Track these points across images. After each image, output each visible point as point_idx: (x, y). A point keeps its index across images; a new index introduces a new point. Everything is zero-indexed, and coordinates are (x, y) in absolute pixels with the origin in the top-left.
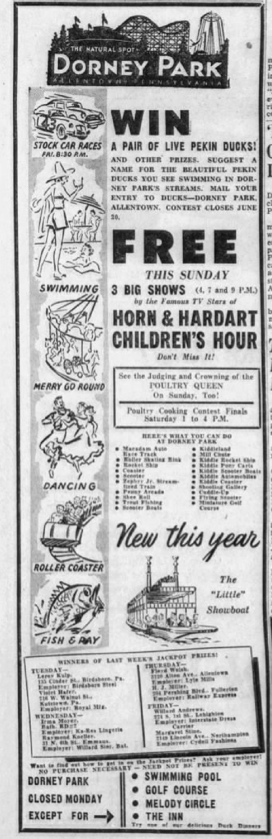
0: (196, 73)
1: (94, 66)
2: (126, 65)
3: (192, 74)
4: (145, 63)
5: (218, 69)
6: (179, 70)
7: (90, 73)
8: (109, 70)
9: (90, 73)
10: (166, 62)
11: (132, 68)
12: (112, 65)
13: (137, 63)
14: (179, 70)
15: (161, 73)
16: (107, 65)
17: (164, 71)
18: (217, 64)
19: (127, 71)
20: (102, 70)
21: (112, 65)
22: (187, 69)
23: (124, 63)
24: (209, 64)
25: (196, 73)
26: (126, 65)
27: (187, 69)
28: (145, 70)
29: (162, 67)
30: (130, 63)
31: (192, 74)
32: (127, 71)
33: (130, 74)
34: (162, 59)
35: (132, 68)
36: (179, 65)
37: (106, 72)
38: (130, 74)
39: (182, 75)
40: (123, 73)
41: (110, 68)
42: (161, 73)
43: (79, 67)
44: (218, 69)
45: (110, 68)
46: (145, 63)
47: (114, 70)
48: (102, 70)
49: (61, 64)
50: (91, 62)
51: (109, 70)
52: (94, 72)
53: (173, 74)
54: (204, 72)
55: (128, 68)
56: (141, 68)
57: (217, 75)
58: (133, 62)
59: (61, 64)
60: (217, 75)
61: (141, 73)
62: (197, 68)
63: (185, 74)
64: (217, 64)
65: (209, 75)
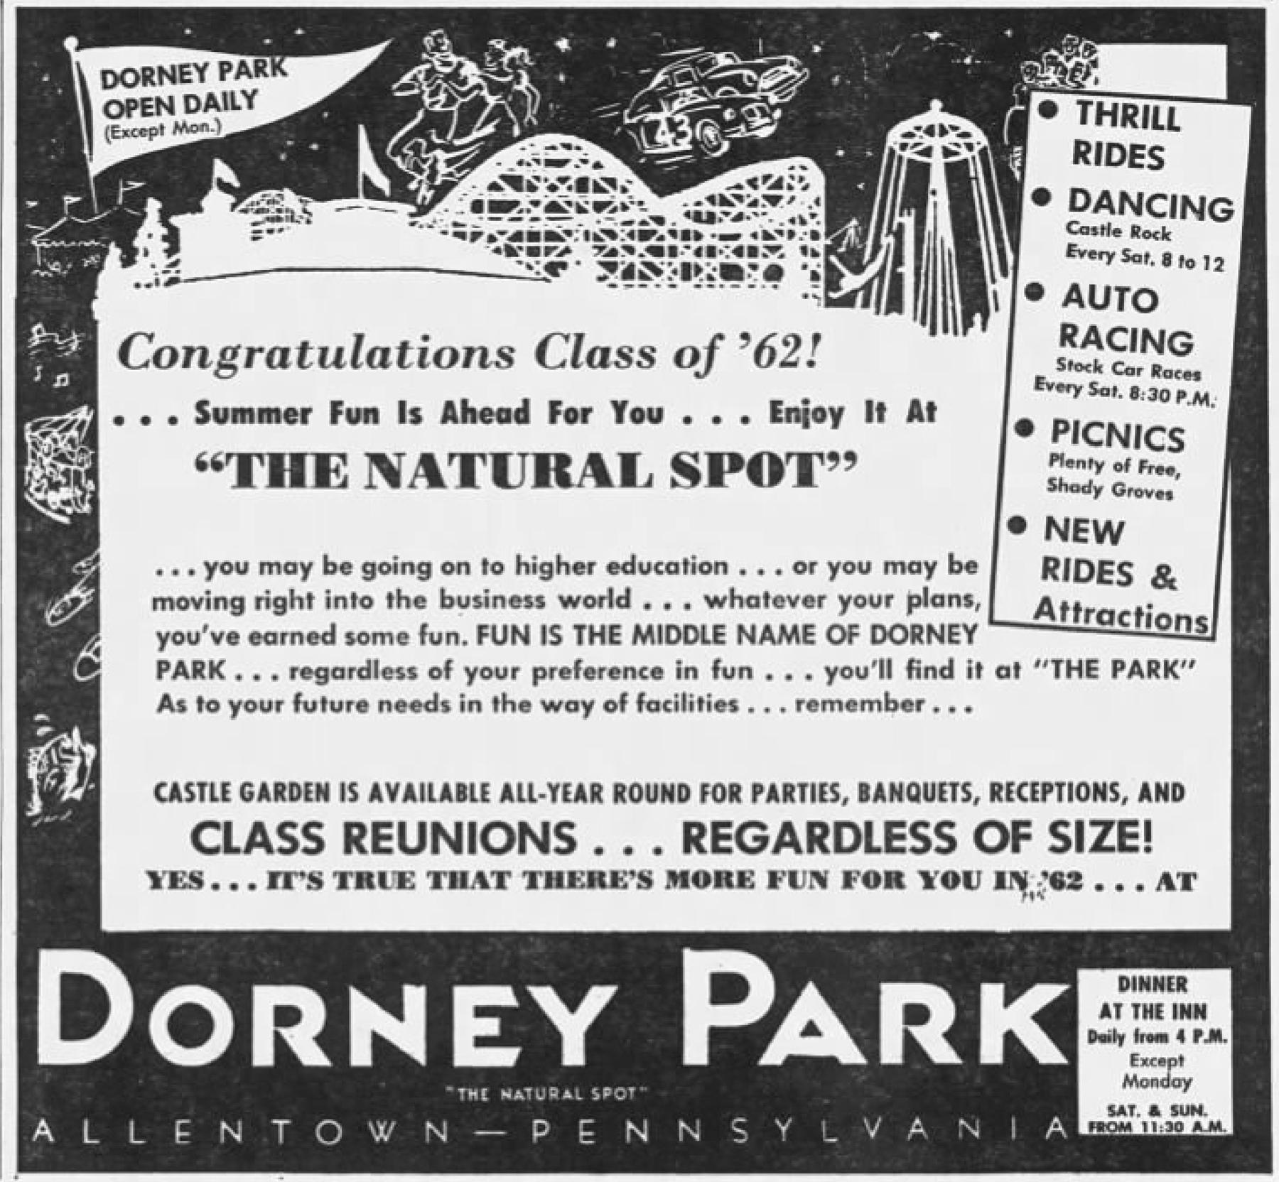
0: (911, 1045)
1: (287, 1016)
2: (481, 1012)
3: (891, 1053)
4: (598, 997)
5: (1045, 1018)
6: (813, 1030)
7: (263, 1055)
8: (380, 1045)
9: (263, 1055)
10: (728, 989)
11: (524, 1026)
12: (397, 1011)
13: (546, 997)
14: (811, 1030)
15: (696, 1052)
16: (366, 1016)
17: (716, 1035)
18: (1044, 994)
19: (481, 1042)
20: (335, 1036)
21: (397, 1011)
22: (863, 1025)
23: (466, 998)
24: (991, 993)
25: (911, 1046)
26: (481, 1012)
27: (863, 1025)
28: (594, 1035)
29: (700, 1019)
30: (503, 996)
31: (891, 1053)
32: (481, 1042)
33: (506, 1057)
34: (698, 968)
35: (524, 1026)
36: (810, 1003)
37: (361, 1056)
38: (506, 1057)
39: (830, 1062)
40: (466, 1055)
41: (388, 1026)
42: (696, 1052)
43: (191, 1026)
44: (1045, 1018)
45: (388, 1026)
46: (598, 997)
47: (410, 1037)
48: (335, 1036)
49: (83, 1007)
50: (266, 998)
51: (380, 1045)
52: (281, 1046)
53: (773, 1056)
54: (964, 1033)
55: (491, 1027)
56: (573, 1027)
57: (1046, 1052)
58: (522, 995)
59: (83, 1007)
60: (1046, 1052)
61: (573, 1054)
62: (917, 1014)
63: (850, 1054)
64: (1044, 994)
65: (991, 1052)
